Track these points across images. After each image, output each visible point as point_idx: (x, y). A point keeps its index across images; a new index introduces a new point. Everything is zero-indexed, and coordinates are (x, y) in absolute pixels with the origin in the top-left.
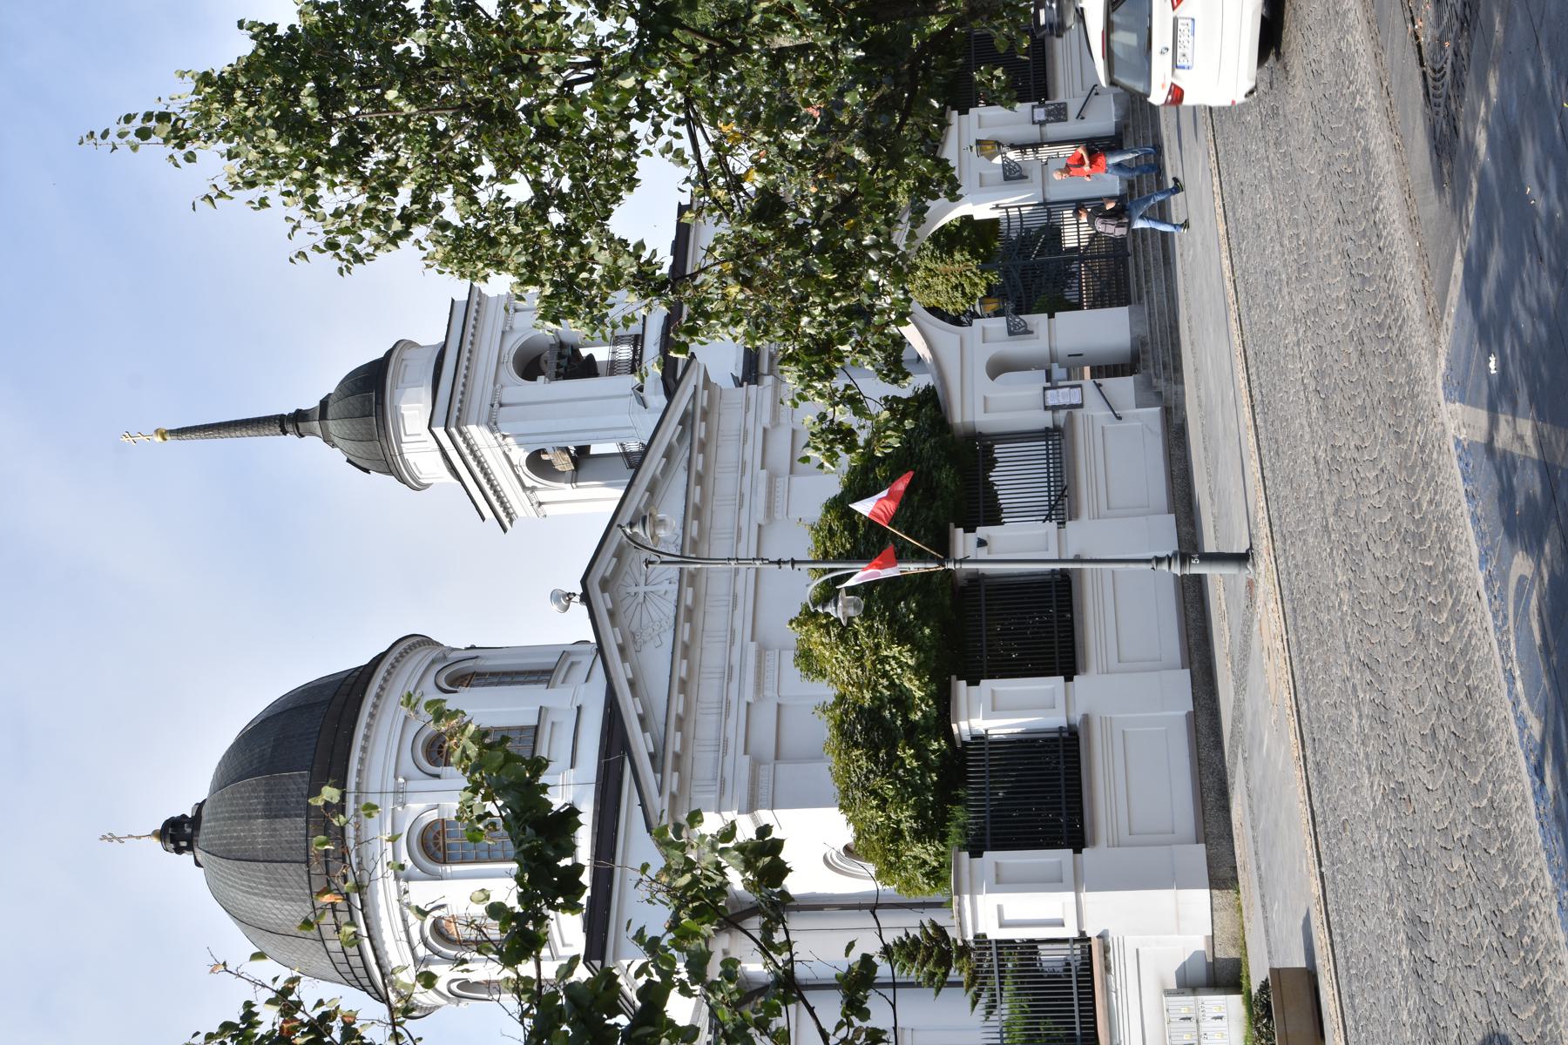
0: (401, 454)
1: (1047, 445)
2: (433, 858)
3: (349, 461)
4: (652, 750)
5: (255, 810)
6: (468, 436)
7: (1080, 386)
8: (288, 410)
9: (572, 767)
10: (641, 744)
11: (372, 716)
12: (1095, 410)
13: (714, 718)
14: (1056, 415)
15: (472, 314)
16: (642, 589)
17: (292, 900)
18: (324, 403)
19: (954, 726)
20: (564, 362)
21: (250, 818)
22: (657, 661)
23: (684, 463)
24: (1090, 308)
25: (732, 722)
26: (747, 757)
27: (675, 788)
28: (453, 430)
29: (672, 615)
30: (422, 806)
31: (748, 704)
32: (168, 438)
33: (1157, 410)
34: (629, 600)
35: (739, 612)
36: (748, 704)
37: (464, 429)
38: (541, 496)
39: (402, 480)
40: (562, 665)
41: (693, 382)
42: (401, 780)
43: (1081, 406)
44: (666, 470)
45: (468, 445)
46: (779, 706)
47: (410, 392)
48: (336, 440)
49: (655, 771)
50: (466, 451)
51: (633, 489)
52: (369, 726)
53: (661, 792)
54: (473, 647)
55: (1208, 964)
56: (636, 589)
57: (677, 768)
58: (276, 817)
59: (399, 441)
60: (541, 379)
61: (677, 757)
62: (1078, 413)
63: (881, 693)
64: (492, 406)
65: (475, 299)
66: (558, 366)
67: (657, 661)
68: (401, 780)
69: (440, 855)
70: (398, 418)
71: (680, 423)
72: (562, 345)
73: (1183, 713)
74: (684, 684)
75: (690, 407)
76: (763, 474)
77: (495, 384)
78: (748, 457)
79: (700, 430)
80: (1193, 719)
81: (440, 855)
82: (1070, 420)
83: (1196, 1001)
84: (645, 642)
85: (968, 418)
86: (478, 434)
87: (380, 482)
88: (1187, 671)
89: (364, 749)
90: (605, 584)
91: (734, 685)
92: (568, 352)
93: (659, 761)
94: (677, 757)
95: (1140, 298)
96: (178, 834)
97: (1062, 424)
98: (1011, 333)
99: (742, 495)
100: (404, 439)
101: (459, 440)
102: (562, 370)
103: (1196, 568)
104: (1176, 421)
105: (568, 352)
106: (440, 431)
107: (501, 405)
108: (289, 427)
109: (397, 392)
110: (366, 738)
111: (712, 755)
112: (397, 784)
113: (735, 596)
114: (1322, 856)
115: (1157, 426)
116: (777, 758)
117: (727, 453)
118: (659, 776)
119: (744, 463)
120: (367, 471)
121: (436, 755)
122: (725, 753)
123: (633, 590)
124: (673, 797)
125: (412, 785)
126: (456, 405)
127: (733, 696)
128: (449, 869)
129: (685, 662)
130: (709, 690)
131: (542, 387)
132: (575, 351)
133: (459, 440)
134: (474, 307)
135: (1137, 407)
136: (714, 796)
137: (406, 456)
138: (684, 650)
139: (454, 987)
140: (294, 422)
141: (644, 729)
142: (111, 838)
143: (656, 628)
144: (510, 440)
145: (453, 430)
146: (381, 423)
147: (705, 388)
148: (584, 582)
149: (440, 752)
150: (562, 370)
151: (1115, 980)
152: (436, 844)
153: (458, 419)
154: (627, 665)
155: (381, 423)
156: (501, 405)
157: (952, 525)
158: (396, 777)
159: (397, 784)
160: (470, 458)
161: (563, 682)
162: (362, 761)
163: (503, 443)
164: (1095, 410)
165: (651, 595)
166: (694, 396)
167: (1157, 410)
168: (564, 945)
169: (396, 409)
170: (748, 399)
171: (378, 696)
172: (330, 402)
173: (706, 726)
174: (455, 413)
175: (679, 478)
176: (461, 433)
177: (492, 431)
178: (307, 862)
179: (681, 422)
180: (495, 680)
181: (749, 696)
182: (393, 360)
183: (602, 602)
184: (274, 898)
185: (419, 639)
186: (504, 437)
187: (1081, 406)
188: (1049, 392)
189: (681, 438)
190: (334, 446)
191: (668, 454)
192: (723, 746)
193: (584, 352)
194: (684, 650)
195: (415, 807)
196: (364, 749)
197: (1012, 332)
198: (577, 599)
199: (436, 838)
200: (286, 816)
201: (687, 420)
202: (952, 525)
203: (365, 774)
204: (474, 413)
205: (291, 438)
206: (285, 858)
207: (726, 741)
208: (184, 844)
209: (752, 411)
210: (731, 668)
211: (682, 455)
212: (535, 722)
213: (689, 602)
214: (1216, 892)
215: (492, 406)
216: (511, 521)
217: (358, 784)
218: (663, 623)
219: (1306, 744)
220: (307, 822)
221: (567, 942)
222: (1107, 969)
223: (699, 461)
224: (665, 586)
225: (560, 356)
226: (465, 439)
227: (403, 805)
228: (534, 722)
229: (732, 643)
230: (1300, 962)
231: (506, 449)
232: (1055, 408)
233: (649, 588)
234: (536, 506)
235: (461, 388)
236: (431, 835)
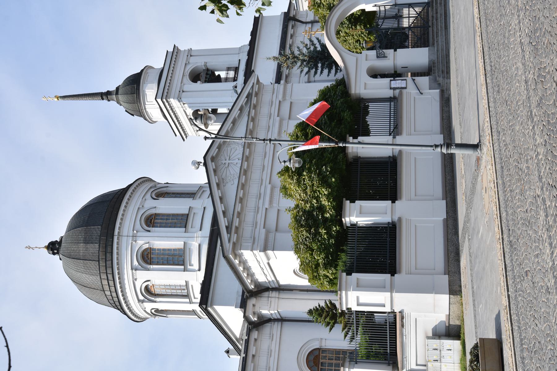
0: (145, 109)
1: (390, 104)
2: (146, 262)
3: (126, 111)
4: (227, 225)
5: (80, 240)
6: (170, 103)
7: (406, 80)
8: (104, 90)
10: (223, 223)
11: (126, 207)
12: (411, 90)
13: (252, 214)
14: (395, 91)
15: (174, 56)
16: (227, 162)
17: (93, 275)
18: (118, 89)
19: (343, 219)
20: (208, 76)
21: (78, 243)
22: (231, 190)
23: (247, 113)
24: (412, 48)
25: (259, 215)
26: (264, 230)
27: (235, 240)
28: (164, 100)
29: (239, 172)
30: (143, 242)
31: (266, 209)
32: (60, 99)
33: (438, 91)
34: (223, 165)
35: (265, 172)
37: (169, 100)
39: (146, 119)
40: (199, 192)
41: (252, 82)
42: (135, 232)
43: (405, 88)
44: (240, 115)
45: (170, 107)
46: (278, 210)
47: (149, 85)
48: (121, 103)
49: (228, 233)
50: (169, 109)
51: (226, 122)
52: (124, 211)
53: (229, 241)
54: (167, 183)
55: (446, 326)
56: (225, 162)
57: (237, 232)
58: (88, 243)
59: (145, 104)
60: (199, 82)
61: (237, 228)
62: (404, 91)
63: (313, 204)
64: (180, 92)
65: (176, 51)
66: (206, 78)
67: (231, 190)
68: (135, 232)
69: (149, 261)
70: (145, 95)
71: (246, 97)
72: (208, 70)
73: (442, 219)
74: (241, 200)
75: (251, 91)
76: (278, 119)
77: (181, 83)
78: (272, 112)
79: (254, 100)
80: (446, 221)
81: (149, 261)
82: (401, 94)
83: (440, 342)
84: (227, 183)
85: (357, 92)
86: (174, 102)
87: (137, 119)
88: (445, 201)
89: (122, 219)
90: (213, 159)
91: (261, 201)
92: (210, 72)
93: (229, 229)
94: (237, 228)
95: (433, 44)
97: (397, 96)
98: (378, 57)
99: (269, 127)
100: (147, 103)
101: (167, 104)
102: (207, 79)
103: (453, 151)
104: (446, 96)
105: (210, 72)
106: (159, 100)
107: (183, 92)
108: (104, 97)
109: (144, 85)
110: (123, 215)
111: (251, 228)
112: (133, 233)
113: (264, 166)
114: (509, 287)
115: (438, 98)
116: (276, 230)
117: (264, 110)
118: (229, 235)
119: (271, 114)
120: (133, 115)
121: (149, 223)
122: (256, 227)
123: (224, 162)
124: (234, 244)
125: (139, 234)
126: (166, 91)
127: (261, 206)
128: (152, 267)
129: (242, 191)
130: (251, 203)
131: (199, 85)
132: (213, 73)
133: (167, 104)
134: (175, 54)
135: (430, 89)
136: (250, 244)
137: (147, 110)
138: (242, 186)
139: (153, 311)
140: (106, 95)
141: (224, 216)
142: (29, 248)
143: (232, 177)
144: (186, 105)
145: (164, 100)
146: (138, 97)
147: (257, 84)
149: (151, 222)
150: (207, 79)
151: (406, 331)
152: (147, 257)
153: (166, 96)
154: (219, 191)
155: (138, 97)
156: (183, 92)
157: (348, 135)
158: (133, 231)
159: (133, 233)
160: (171, 111)
161: (199, 198)
162: (121, 224)
163: (183, 106)
164: (411, 90)
165: (230, 164)
166: (253, 87)
167: (438, 91)
168: (195, 298)
169: (144, 91)
170: (274, 89)
171: (129, 199)
172: (120, 88)
173: (249, 217)
174: (165, 94)
175: (245, 119)
176: (167, 101)
177: (179, 101)
178: (99, 261)
179: (247, 97)
180: (174, 196)
181: (267, 206)
183: (211, 166)
184: (86, 274)
185: (146, 179)
186: (184, 104)
187: (405, 88)
188: (392, 82)
190: (121, 105)
191: (241, 109)
192: (255, 224)
193: (217, 73)
194: (242, 186)
195: (140, 242)
196: (122, 219)
198: (202, 164)
199: (147, 255)
200: (91, 243)
201: (249, 96)
202: (348, 135)
203: (122, 229)
204: (172, 94)
205: (105, 101)
206: (91, 259)
207: (256, 223)
208: (56, 251)
209: (275, 95)
210: (260, 194)
212: (188, 213)
213: (245, 167)
214: (452, 296)
215: (180, 92)
216: (186, 137)
217: (119, 233)
218: (235, 175)
219: (504, 232)
220: (99, 246)
221: (196, 297)
222: (403, 326)
224: (237, 161)
225: (207, 74)
226: (169, 104)
227: (136, 241)
228: (187, 212)
229: (261, 184)
230: (492, 335)
231: (185, 109)
232: (394, 89)
233: (230, 162)
234: (196, 131)
236: (146, 253)
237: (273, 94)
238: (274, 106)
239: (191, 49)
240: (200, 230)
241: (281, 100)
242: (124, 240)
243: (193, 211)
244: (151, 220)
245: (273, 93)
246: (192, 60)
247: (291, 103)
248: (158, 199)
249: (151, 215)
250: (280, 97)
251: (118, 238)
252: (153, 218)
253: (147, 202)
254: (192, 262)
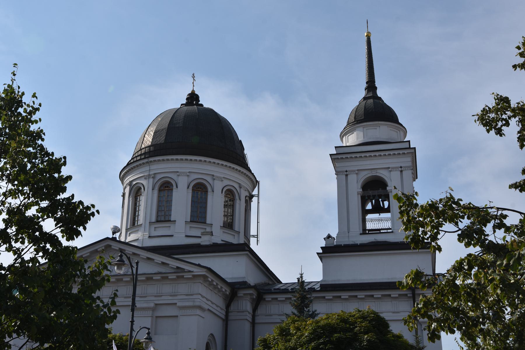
30: (145, 185)
75: (185, 270)
78: (163, 298)
79: (171, 276)
89: (163, 160)
96: (193, 98)
110: (168, 160)
112: (151, 175)
117: (167, 288)
125: (151, 180)
140: (371, 86)
147: (195, 276)
149: (166, 187)
166: (190, 271)
179: (178, 268)
195: (144, 182)
211: (163, 270)
217: (151, 162)
223: (158, 277)
227: (145, 179)
237: (185, 295)
241: (178, 305)
242: (147, 168)
243: (172, 225)
244: (168, 187)
245: (187, 295)
247: (177, 316)
248: (188, 188)
249: (172, 185)
250: (179, 304)
251: (147, 162)
252: (169, 188)
253: (186, 178)
254: (131, 235)
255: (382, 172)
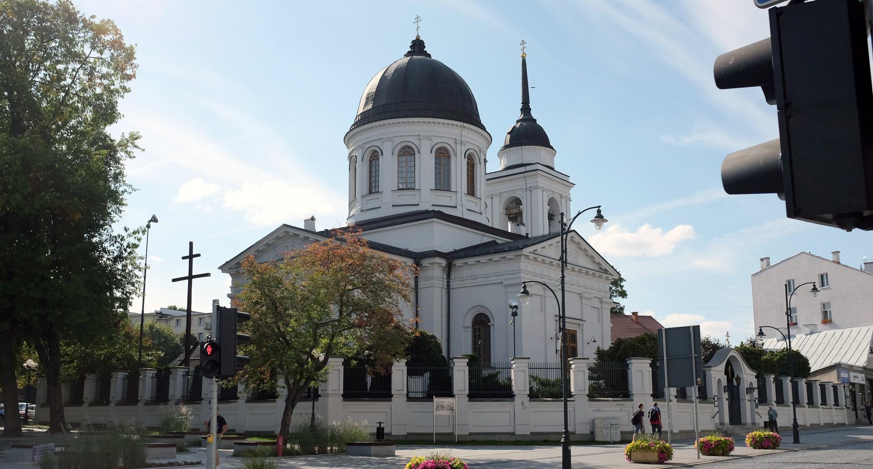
8: (531, 105)
9: (468, 209)
36: (502, 283)
38: (496, 200)
44: (594, 262)
79: (604, 275)
82: (712, 403)
96: (418, 46)
97: (708, 400)
140: (526, 108)
148: (574, 231)
156: (543, 191)
166: (611, 274)
182: (549, 149)
189: (601, 269)
191: (599, 264)
197: (724, 387)
205: (520, 106)
223: (598, 274)
235: (553, 179)
238: (598, 293)
239: (571, 200)
240: (468, 209)
246: (564, 200)
255: (556, 194)
